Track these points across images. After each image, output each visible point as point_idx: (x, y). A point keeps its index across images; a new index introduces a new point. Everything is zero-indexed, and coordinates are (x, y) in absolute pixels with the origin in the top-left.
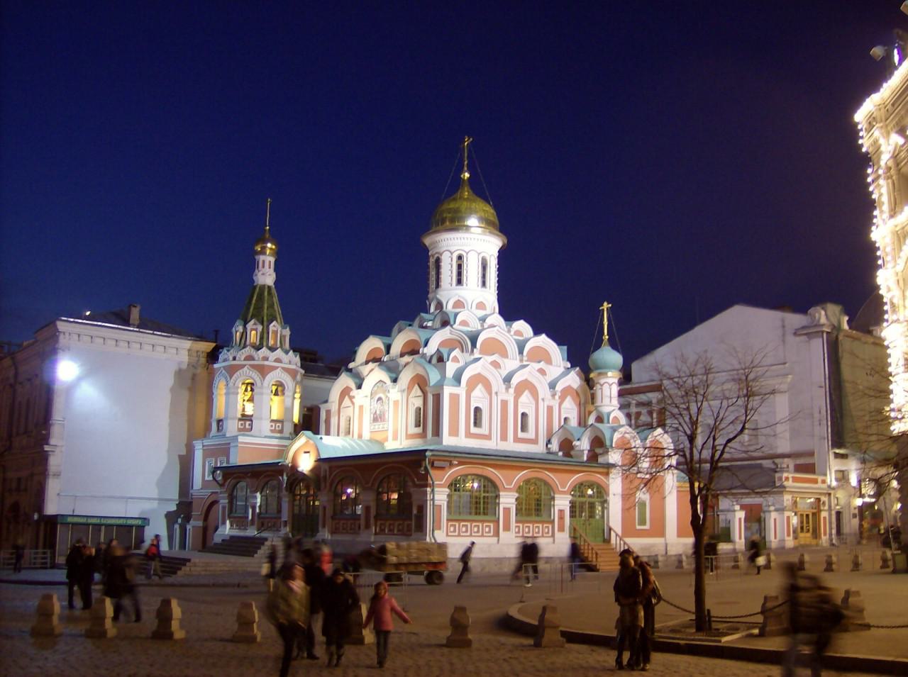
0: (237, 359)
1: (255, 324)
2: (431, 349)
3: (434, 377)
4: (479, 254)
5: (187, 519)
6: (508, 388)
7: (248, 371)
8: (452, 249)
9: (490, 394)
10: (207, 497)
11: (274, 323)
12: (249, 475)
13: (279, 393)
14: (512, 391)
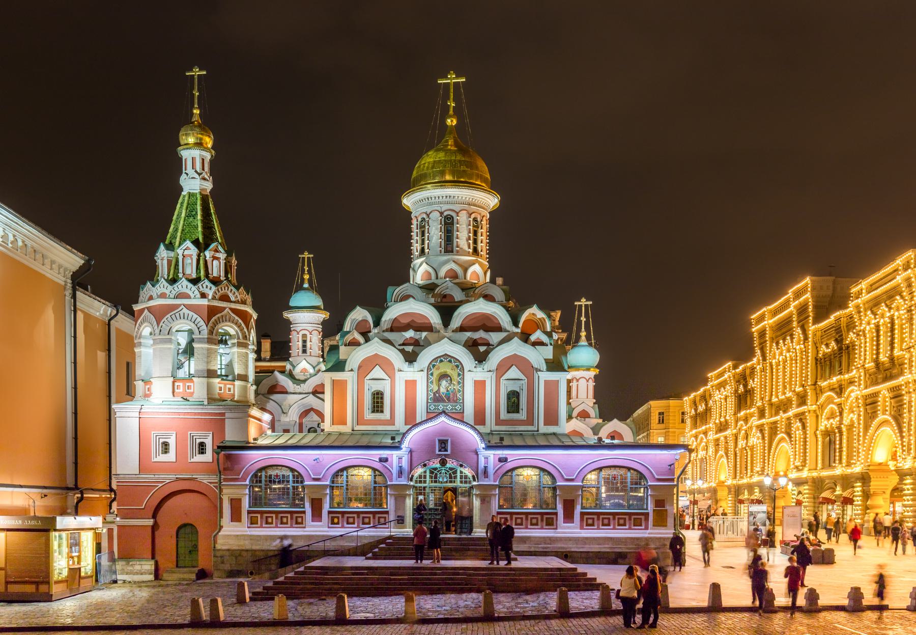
10: (161, 485)
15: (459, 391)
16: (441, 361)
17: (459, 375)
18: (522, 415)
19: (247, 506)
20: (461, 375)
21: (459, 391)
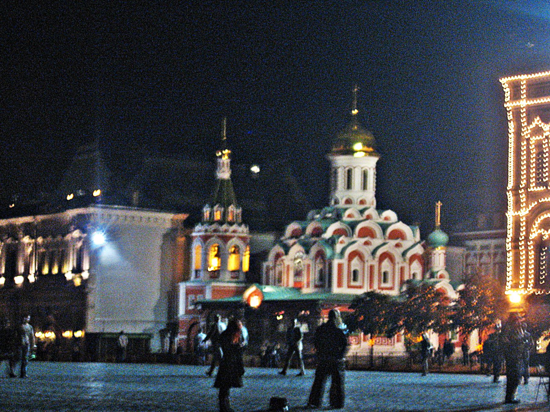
2: (328, 235)
3: (328, 252)
5: (174, 334)
6: (374, 259)
11: (232, 206)
13: (236, 252)
14: (377, 259)
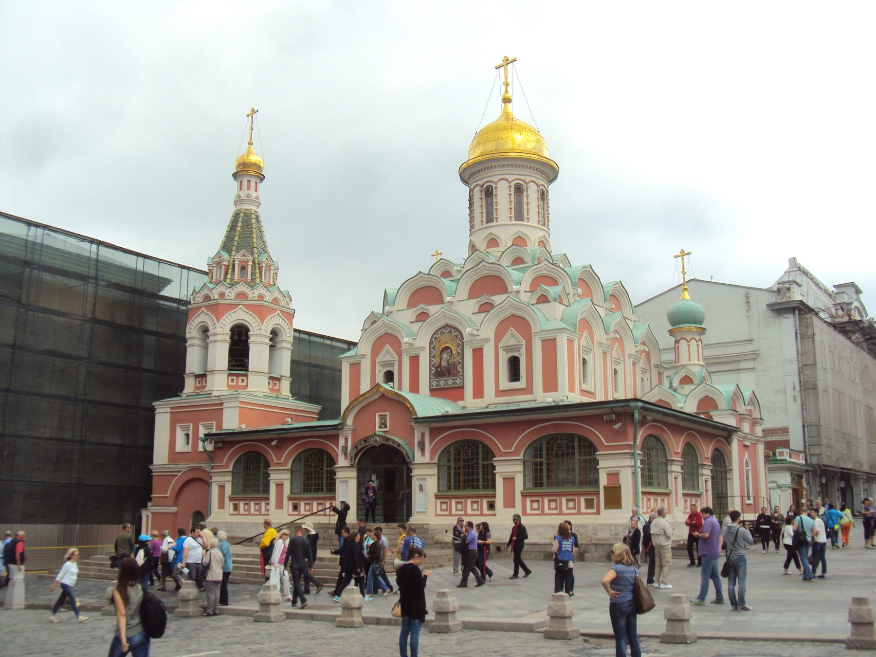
0: (226, 297)
1: (244, 255)
4: (538, 186)
7: (240, 312)
8: (510, 178)
9: (593, 344)
10: (179, 474)
12: (274, 443)
15: (459, 363)
16: (442, 333)
17: (459, 345)
18: (522, 384)
19: (230, 493)
20: (462, 346)
21: (459, 363)
